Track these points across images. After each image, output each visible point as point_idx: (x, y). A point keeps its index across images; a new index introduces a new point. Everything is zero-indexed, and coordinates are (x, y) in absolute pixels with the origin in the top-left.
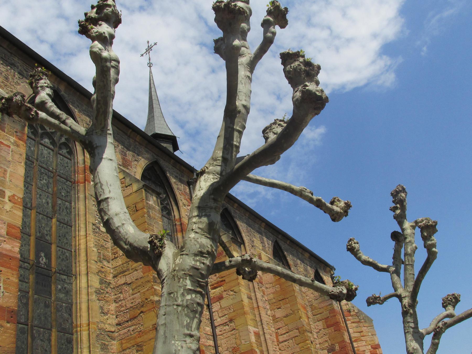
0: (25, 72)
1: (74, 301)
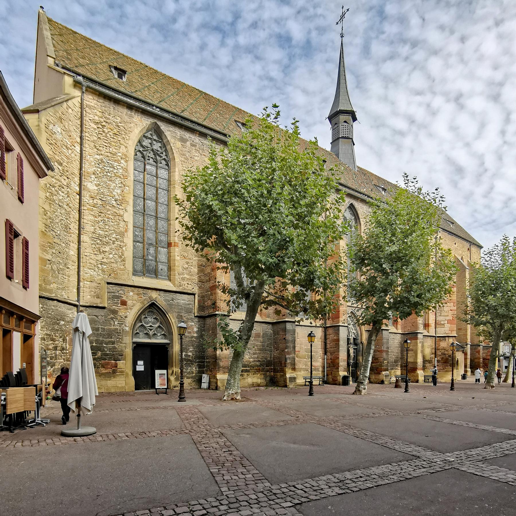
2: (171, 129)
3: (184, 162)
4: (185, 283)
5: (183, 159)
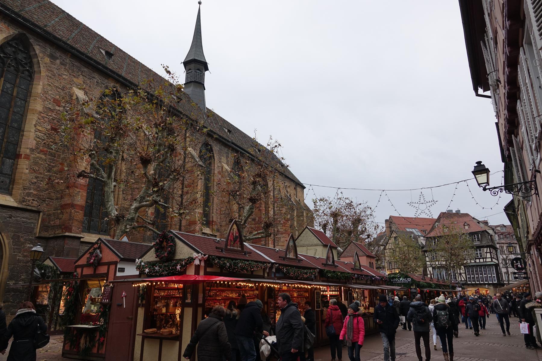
0: (99, 80)
3: (50, 77)
4: (29, 198)
5: (50, 75)
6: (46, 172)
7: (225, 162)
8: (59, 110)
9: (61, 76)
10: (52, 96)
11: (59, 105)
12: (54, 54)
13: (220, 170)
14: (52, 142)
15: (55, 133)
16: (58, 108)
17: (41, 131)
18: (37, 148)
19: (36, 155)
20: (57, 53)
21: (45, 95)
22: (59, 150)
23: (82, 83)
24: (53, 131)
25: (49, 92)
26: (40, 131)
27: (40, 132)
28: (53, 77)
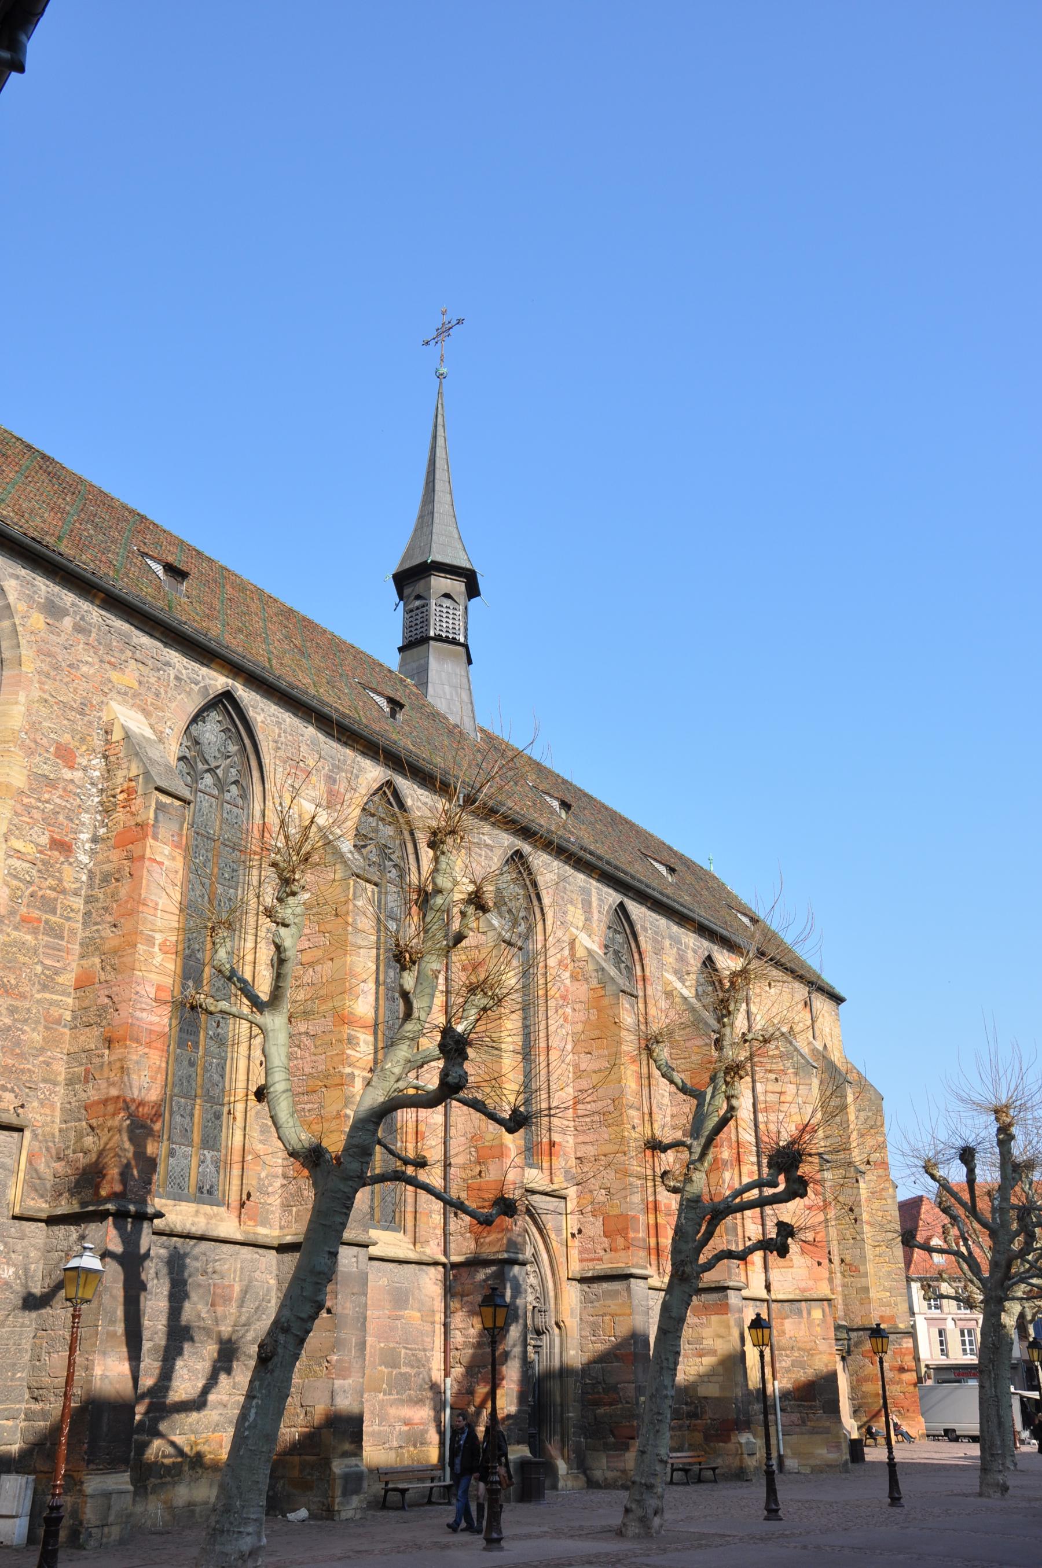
1: (229, 1055)
2: (23, 572)
6: (39, 991)
7: (581, 925)
8: (72, 781)
9: (78, 668)
10: (52, 735)
11: (70, 764)
12: (56, 600)
13: (566, 952)
14: (54, 890)
15: (62, 859)
16: (67, 774)
17: (24, 854)
18: (13, 913)
19: (8, 935)
20: (64, 597)
21: (32, 736)
22: (71, 915)
23: (136, 685)
24: (56, 853)
25: (44, 724)
26: (18, 854)
27: (19, 858)
28: (53, 673)
